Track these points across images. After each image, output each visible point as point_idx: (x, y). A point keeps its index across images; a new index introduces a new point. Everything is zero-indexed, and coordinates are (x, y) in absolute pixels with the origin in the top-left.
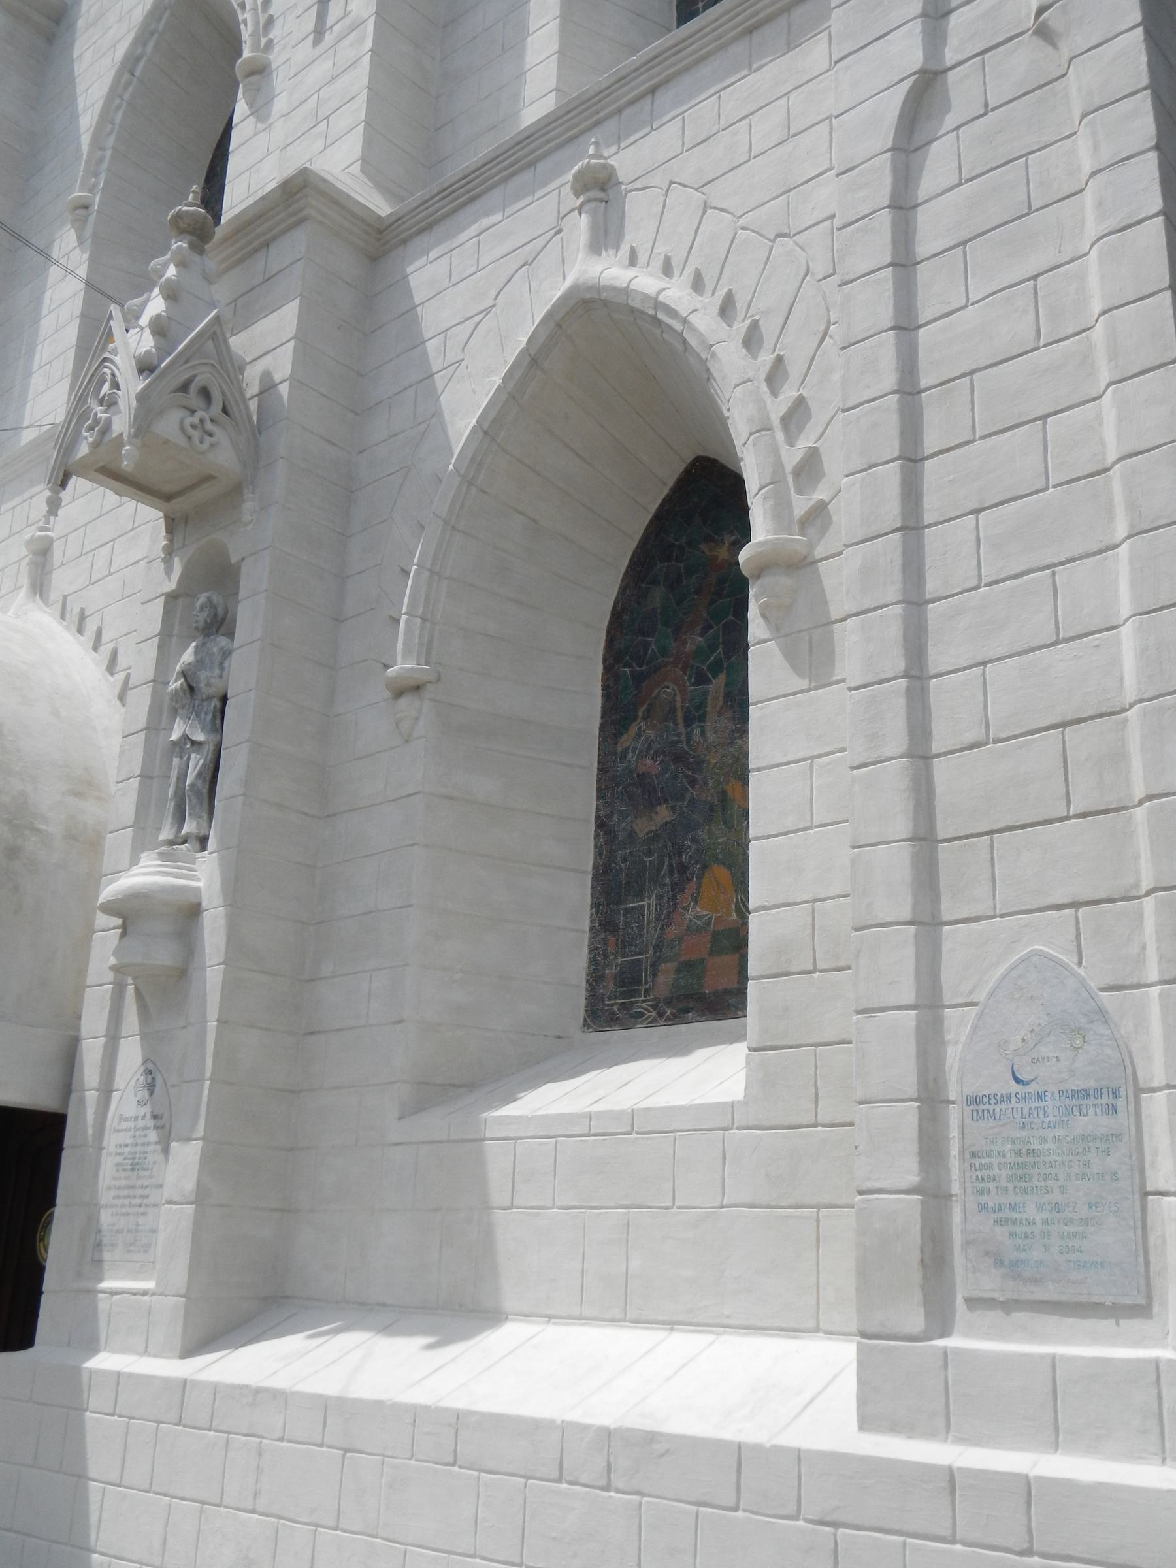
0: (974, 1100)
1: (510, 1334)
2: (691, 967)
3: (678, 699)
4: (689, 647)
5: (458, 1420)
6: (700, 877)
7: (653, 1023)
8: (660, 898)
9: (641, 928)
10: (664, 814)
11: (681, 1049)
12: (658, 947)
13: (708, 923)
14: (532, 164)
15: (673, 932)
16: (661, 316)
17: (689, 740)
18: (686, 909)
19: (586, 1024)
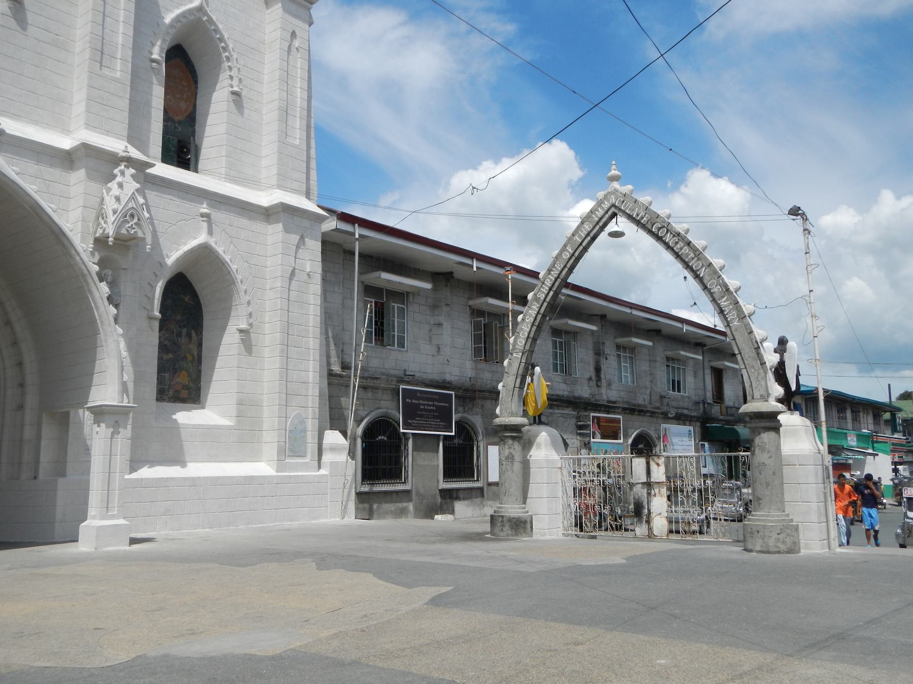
0: (290, 431)
1: (190, 465)
2: (177, 391)
3: (175, 330)
4: (178, 318)
5: (193, 479)
6: (180, 372)
7: (168, 402)
8: (170, 374)
9: (165, 380)
10: (170, 356)
11: (189, 410)
12: (169, 385)
13: (181, 383)
14: (188, 193)
15: (173, 383)
16: (226, 264)
17: (177, 339)
18: (176, 379)
19: (158, 400)
